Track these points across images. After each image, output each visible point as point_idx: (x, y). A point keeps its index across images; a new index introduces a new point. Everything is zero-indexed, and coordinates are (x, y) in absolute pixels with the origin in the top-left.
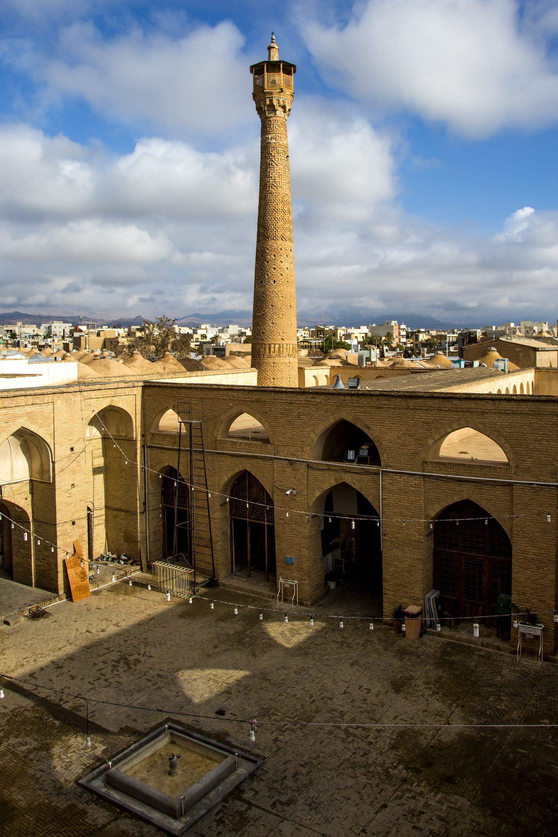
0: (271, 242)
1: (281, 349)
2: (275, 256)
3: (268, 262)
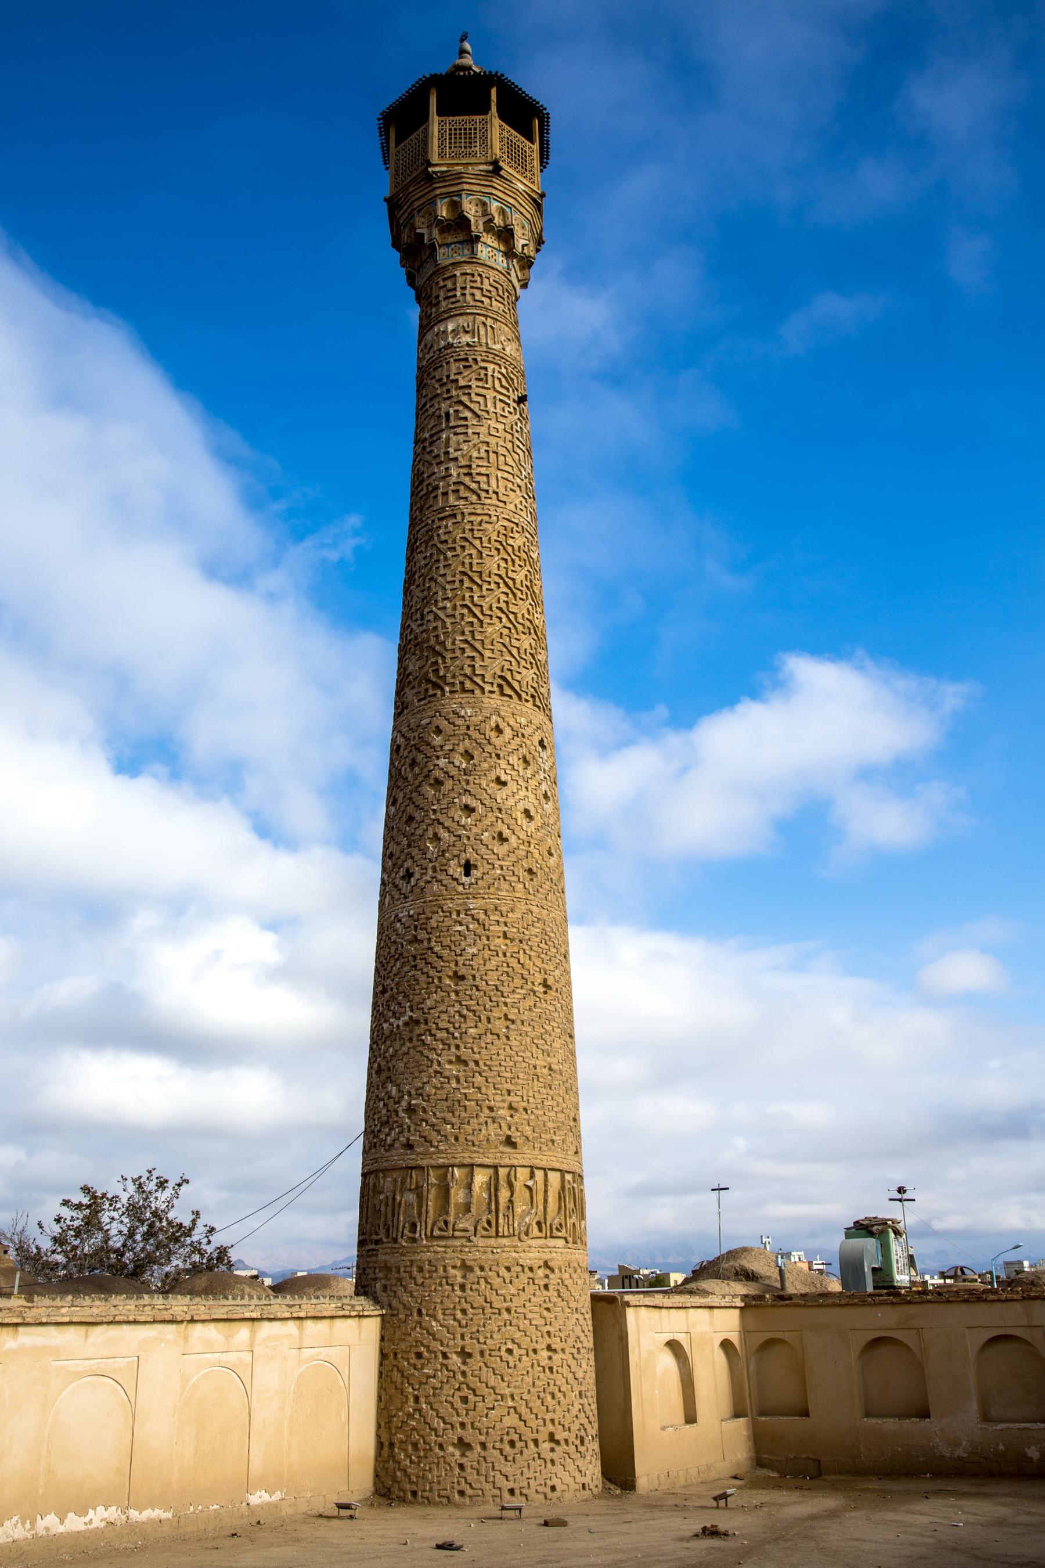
0: (452, 703)
1: (504, 1194)
2: (468, 755)
3: (438, 783)
